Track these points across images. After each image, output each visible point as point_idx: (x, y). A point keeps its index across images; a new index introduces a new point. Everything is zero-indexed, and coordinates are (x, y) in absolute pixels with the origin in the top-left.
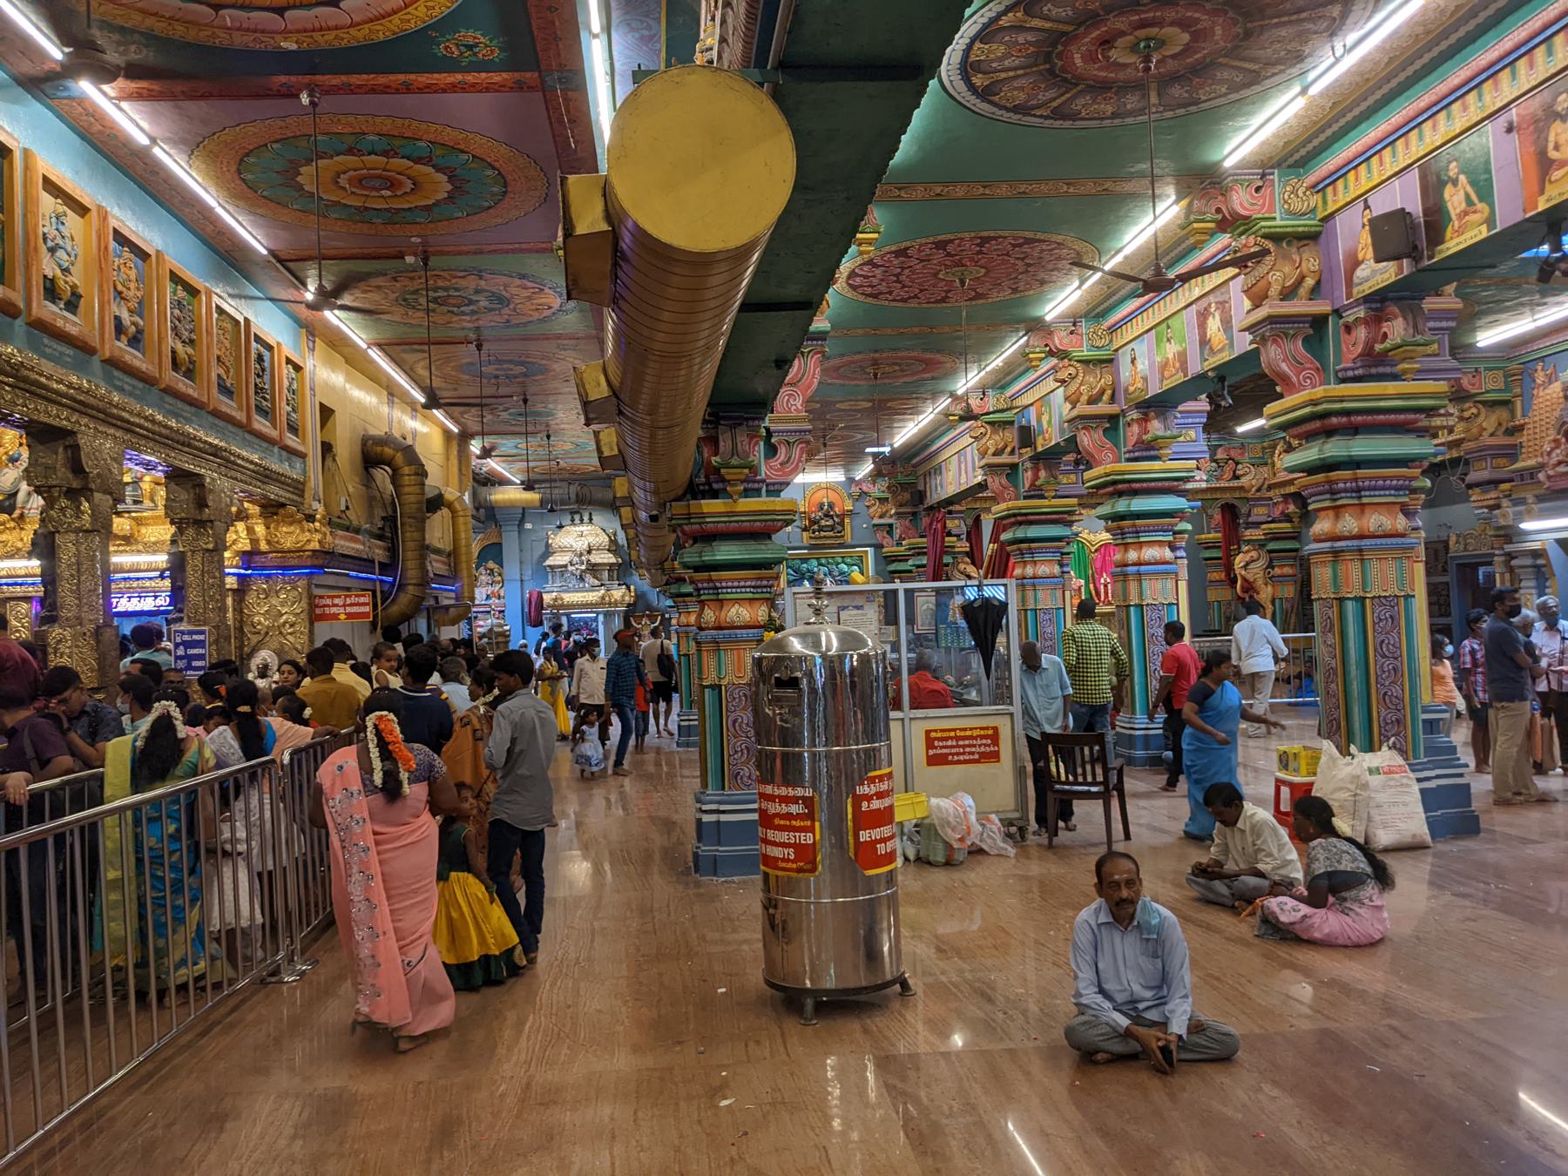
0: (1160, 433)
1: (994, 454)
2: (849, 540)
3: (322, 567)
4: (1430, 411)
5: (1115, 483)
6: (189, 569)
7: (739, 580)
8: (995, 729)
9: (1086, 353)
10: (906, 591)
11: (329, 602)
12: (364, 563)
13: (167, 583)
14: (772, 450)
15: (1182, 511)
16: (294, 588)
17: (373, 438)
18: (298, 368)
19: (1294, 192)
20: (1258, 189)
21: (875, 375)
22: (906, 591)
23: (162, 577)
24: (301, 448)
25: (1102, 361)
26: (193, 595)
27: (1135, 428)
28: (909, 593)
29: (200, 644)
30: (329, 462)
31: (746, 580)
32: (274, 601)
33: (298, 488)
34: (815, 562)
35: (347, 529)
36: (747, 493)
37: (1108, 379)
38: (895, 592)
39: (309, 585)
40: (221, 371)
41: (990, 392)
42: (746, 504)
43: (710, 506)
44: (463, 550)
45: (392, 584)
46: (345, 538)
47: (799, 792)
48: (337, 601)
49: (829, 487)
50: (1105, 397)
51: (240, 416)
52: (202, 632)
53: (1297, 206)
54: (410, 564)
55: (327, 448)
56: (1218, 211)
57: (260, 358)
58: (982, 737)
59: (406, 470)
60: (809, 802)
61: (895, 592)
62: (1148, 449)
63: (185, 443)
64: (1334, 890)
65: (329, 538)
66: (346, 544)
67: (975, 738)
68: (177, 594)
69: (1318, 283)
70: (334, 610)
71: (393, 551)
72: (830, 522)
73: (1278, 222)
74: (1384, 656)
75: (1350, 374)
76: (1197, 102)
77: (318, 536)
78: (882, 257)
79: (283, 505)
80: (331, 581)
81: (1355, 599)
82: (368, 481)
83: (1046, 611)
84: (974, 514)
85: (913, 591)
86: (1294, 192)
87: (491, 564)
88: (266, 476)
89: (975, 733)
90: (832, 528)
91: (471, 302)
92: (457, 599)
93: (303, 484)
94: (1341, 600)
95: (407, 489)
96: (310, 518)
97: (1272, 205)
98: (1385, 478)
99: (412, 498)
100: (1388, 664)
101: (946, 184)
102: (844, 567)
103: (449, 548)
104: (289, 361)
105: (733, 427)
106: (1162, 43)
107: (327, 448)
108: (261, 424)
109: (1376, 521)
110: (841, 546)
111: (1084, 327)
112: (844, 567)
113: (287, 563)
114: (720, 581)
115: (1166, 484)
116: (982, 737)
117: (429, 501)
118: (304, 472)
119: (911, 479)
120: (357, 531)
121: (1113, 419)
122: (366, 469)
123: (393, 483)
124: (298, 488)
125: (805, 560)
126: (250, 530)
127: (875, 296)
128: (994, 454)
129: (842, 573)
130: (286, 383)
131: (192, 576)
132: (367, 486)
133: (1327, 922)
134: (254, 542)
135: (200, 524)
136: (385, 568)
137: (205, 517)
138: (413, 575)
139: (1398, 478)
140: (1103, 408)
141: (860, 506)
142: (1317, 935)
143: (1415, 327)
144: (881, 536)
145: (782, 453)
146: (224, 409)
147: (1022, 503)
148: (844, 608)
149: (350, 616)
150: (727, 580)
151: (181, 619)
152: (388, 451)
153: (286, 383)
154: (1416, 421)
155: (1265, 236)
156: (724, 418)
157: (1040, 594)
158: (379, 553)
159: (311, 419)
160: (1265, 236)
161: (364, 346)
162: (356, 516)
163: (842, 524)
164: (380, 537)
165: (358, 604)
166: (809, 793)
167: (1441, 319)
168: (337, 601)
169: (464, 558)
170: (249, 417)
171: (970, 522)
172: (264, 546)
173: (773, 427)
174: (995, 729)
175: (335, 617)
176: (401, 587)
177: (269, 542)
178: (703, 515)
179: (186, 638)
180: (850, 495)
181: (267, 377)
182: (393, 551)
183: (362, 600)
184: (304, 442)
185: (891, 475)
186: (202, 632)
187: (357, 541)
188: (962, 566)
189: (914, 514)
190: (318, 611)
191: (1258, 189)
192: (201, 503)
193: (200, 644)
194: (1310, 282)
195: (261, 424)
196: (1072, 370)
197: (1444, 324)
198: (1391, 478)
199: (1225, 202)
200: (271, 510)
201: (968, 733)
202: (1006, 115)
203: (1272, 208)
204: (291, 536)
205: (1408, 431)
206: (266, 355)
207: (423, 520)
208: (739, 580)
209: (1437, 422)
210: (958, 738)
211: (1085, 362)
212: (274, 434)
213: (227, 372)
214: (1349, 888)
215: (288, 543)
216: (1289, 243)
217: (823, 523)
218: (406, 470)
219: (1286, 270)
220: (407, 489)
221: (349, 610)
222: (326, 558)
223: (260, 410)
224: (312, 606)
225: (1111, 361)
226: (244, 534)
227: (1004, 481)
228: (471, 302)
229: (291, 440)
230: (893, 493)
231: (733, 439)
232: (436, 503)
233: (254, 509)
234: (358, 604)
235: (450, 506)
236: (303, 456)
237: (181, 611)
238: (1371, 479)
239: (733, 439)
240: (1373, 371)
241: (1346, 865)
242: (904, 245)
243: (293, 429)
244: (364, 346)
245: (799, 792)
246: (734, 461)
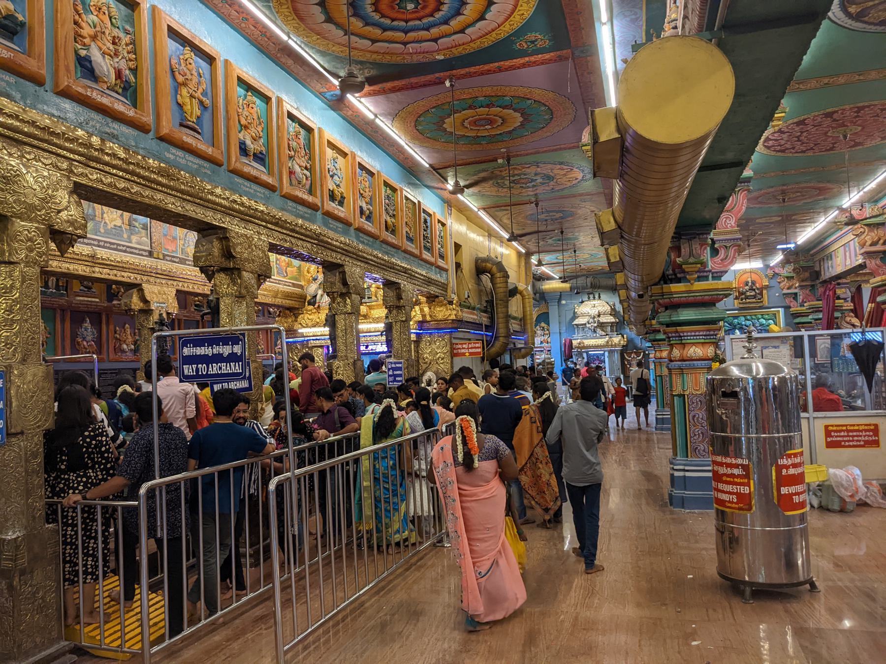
1: (871, 245)
3: (456, 328)
6: (394, 331)
7: (695, 331)
8: (876, 426)
10: (809, 336)
11: (460, 346)
12: (477, 326)
13: (384, 338)
14: (715, 252)
16: (443, 340)
18: (443, 225)
21: (784, 200)
22: (809, 336)
23: (382, 335)
26: (396, 344)
28: (812, 339)
29: (400, 369)
30: (459, 272)
31: (699, 331)
32: (434, 346)
33: (444, 287)
34: (743, 319)
35: (469, 308)
36: (699, 279)
38: (801, 337)
39: (451, 338)
41: (867, 205)
43: (675, 287)
44: (528, 317)
46: (468, 313)
47: (739, 461)
48: (464, 346)
49: (752, 272)
51: (417, 252)
52: (400, 363)
54: (501, 325)
55: (458, 266)
58: (866, 431)
59: (498, 275)
60: (745, 468)
61: (801, 337)
63: (391, 267)
65: (460, 313)
66: (468, 316)
67: (861, 431)
68: (389, 343)
70: (463, 351)
71: (492, 318)
72: (753, 293)
77: (454, 312)
79: (437, 297)
80: (461, 335)
82: (478, 281)
84: (856, 285)
85: (815, 336)
87: (543, 324)
88: (429, 282)
89: (861, 428)
90: (755, 297)
91: (533, 180)
92: (525, 344)
95: (498, 285)
96: (451, 303)
99: (501, 290)
102: (763, 321)
104: (439, 221)
105: (690, 240)
107: (458, 266)
108: (426, 255)
110: (761, 308)
112: (763, 321)
114: (683, 332)
116: (866, 431)
117: (510, 291)
118: (447, 279)
119: (810, 264)
120: (474, 309)
122: (478, 275)
123: (492, 282)
124: (444, 287)
125: (736, 317)
126: (422, 310)
127: (783, 151)
128: (871, 245)
129: (761, 325)
131: (395, 334)
132: (478, 284)
134: (424, 316)
135: (399, 308)
137: (401, 304)
138: (502, 331)
141: (774, 282)
146: (409, 249)
148: (766, 348)
149: (471, 354)
150: (687, 332)
151: (391, 356)
152: (489, 265)
153: (438, 233)
156: (684, 235)
158: (485, 320)
161: (476, 210)
162: (473, 301)
163: (761, 294)
164: (485, 312)
165: (475, 348)
166: (746, 462)
168: (464, 346)
169: (529, 322)
171: (853, 290)
172: (428, 318)
173: (716, 238)
174: (876, 426)
175: (464, 354)
177: (431, 316)
178: (671, 293)
179: (393, 366)
180: (766, 276)
181: (429, 231)
182: (492, 318)
183: (477, 345)
184: (447, 263)
185: (795, 262)
186: (400, 363)
187: (473, 314)
188: (848, 319)
189: (813, 286)
190: (455, 351)
192: (399, 297)
193: (400, 369)
195: (426, 255)
200: (432, 299)
201: (856, 428)
204: (443, 313)
207: (507, 302)
208: (695, 331)
210: (848, 431)
212: (433, 260)
213: (410, 230)
217: (748, 294)
218: (498, 275)
220: (498, 285)
221: (470, 350)
222: (459, 323)
224: (452, 349)
226: (419, 312)
227: (878, 262)
228: (533, 180)
229: (441, 263)
230: (797, 273)
231: (690, 247)
232: (514, 292)
234: (475, 348)
235: (521, 293)
236: (446, 270)
237: (391, 352)
239: (690, 247)
243: (442, 257)
244: (476, 210)
245: (739, 461)
246: (691, 260)
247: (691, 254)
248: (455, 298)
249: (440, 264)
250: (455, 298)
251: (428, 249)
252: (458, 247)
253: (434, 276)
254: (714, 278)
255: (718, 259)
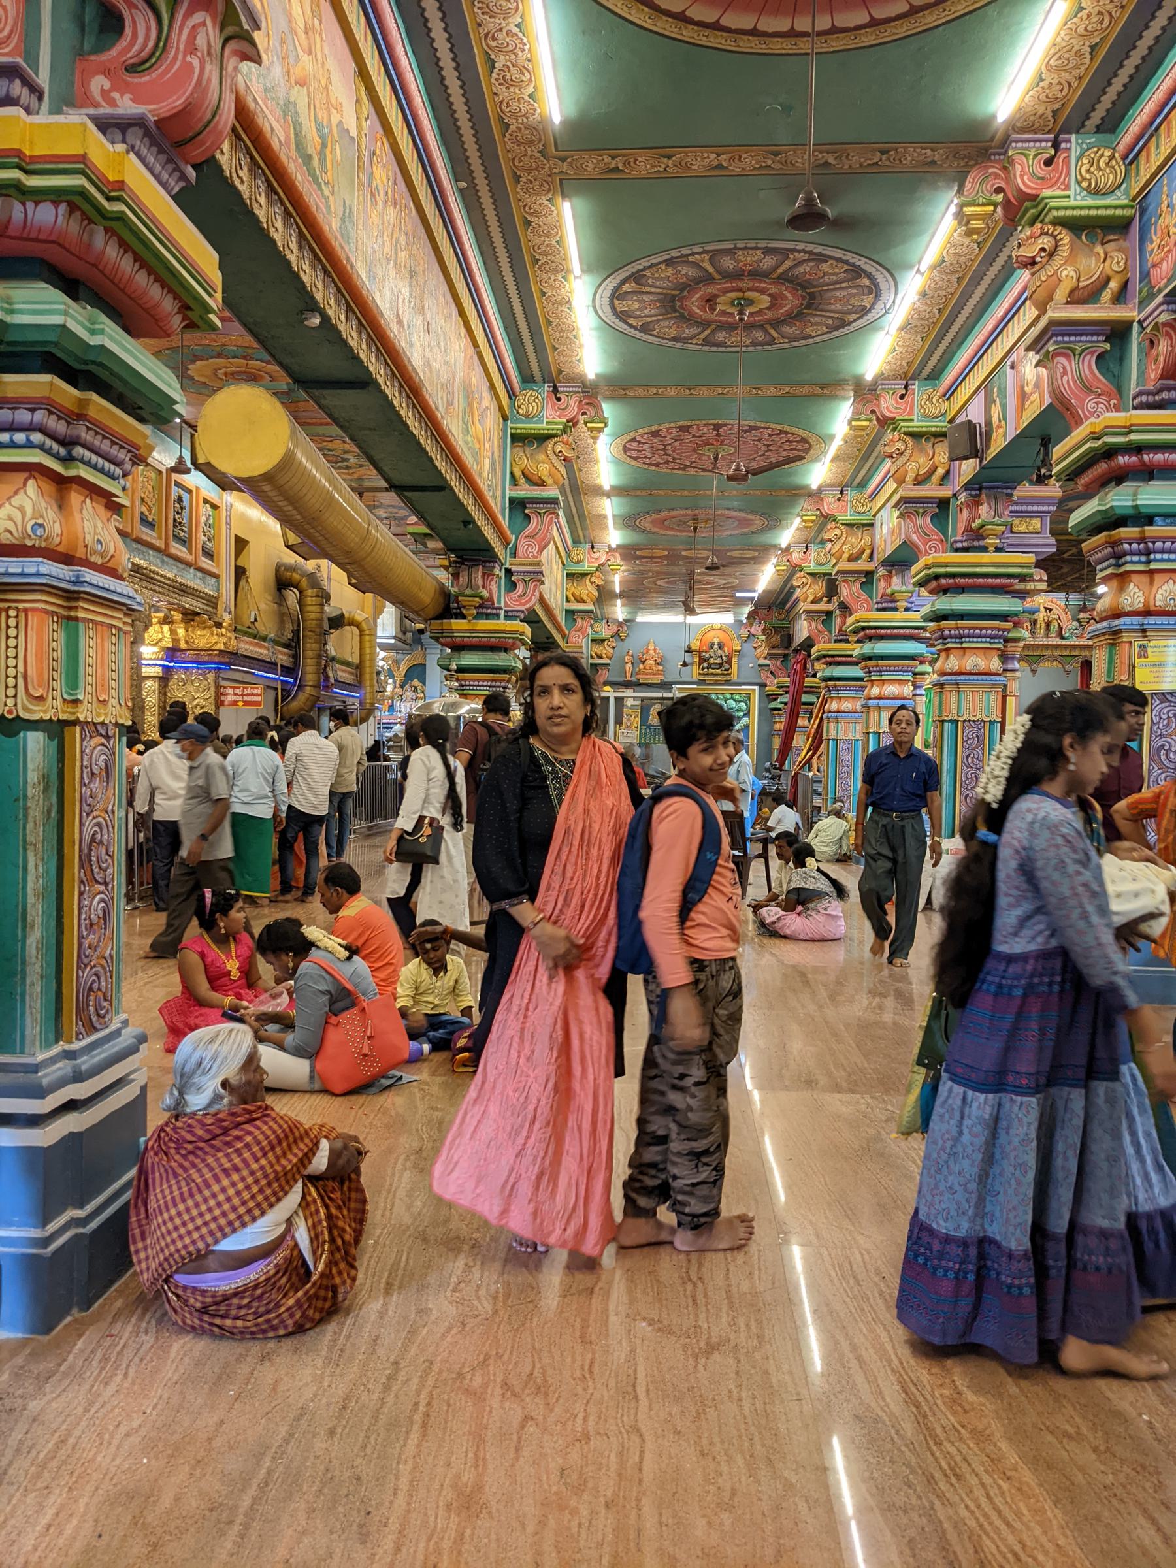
0: (896, 588)
2: (735, 678)
3: (228, 664)
4: (1023, 578)
5: (864, 628)
9: (849, 517)
10: (617, 698)
12: (270, 666)
14: (512, 586)
15: (921, 655)
16: (206, 679)
17: (284, 565)
18: (215, 507)
19: (930, 399)
20: (902, 397)
22: (617, 698)
24: (215, 570)
25: (864, 525)
27: (882, 584)
28: (620, 701)
30: (243, 583)
32: (190, 688)
33: (213, 602)
35: (255, 637)
36: (479, 616)
37: (867, 540)
39: (217, 677)
40: (144, 509)
41: (812, 547)
42: (483, 624)
43: (457, 624)
44: (367, 664)
45: (294, 684)
50: (865, 556)
51: (160, 544)
53: (932, 410)
55: (240, 573)
56: (873, 412)
57: (180, 500)
59: (309, 592)
62: (889, 602)
64: (803, 903)
65: (234, 642)
66: (247, 647)
69: (948, 472)
71: (296, 657)
72: (718, 661)
73: (915, 423)
74: (969, 767)
75: (959, 545)
76: (810, 337)
77: (224, 640)
78: (642, 436)
80: (237, 676)
81: (951, 721)
82: (280, 600)
83: (845, 741)
86: (930, 399)
87: (416, 682)
88: (184, 590)
90: (720, 666)
91: (344, 460)
93: (217, 598)
94: (943, 721)
95: (309, 608)
96: (219, 625)
97: (912, 408)
98: (981, 629)
99: (313, 616)
100: (971, 773)
101: (658, 386)
103: (357, 661)
104: (206, 501)
105: (471, 567)
106: (751, 302)
107: (240, 573)
108: (177, 549)
109: (974, 661)
110: (727, 683)
111: (849, 495)
113: (201, 659)
115: (908, 631)
117: (331, 620)
118: (218, 590)
119: (785, 624)
120: (264, 639)
121: (869, 574)
122: (279, 590)
124: (213, 602)
126: (173, 632)
130: (203, 519)
132: (280, 604)
133: (793, 923)
134: (176, 641)
136: (287, 671)
138: (310, 677)
139: (993, 629)
140: (862, 565)
142: (788, 932)
143: (996, 511)
144: (764, 676)
145: (520, 586)
146: (145, 537)
147: (833, 645)
149: (246, 703)
152: (296, 576)
153: (203, 519)
154: (1011, 585)
155: (906, 434)
157: (841, 726)
158: (283, 657)
159: (226, 549)
160: (906, 434)
163: (729, 662)
164: (287, 646)
167: (1043, 504)
169: (368, 670)
170: (167, 544)
172: (183, 645)
176: (301, 687)
180: (739, 637)
181: (185, 514)
182: (296, 657)
185: (765, 619)
187: (261, 647)
189: (785, 656)
191: (902, 397)
194: (941, 471)
195: (177, 549)
196: (838, 532)
197: (1046, 508)
198: (987, 629)
199: (879, 406)
200: (190, 616)
202: (671, 344)
203: (911, 413)
204: (204, 638)
205: (1007, 592)
206: (186, 497)
207: (326, 633)
209: (1030, 586)
211: (850, 525)
212: (190, 558)
213: (150, 510)
214: (810, 901)
215: (201, 644)
216: (927, 440)
218: (309, 592)
219: (921, 461)
220: (309, 608)
222: (231, 658)
223: (177, 538)
225: (872, 525)
226: (167, 634)
227: (820, 625)
228: (344, 460)
229: (205, 563)
230: (768, 636)
232: (338, 622)
233: (177, 616)
235: (353, 623)
236: (217, 576)
238: (970, 628)
240: (976, 543)
241: (810, 885)
242: (654, 428)
243: (209, 554)
246: (468, 592)
247: (469, 584)
248: (227, 618)
249: (204, 566)
250: (227, 618)
251: (182, 541)
252: (241, 544)
253: (191, 579)
254: (507, 617)
255: (515, 595)
